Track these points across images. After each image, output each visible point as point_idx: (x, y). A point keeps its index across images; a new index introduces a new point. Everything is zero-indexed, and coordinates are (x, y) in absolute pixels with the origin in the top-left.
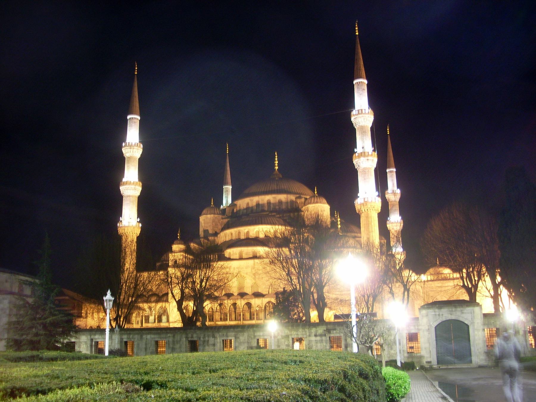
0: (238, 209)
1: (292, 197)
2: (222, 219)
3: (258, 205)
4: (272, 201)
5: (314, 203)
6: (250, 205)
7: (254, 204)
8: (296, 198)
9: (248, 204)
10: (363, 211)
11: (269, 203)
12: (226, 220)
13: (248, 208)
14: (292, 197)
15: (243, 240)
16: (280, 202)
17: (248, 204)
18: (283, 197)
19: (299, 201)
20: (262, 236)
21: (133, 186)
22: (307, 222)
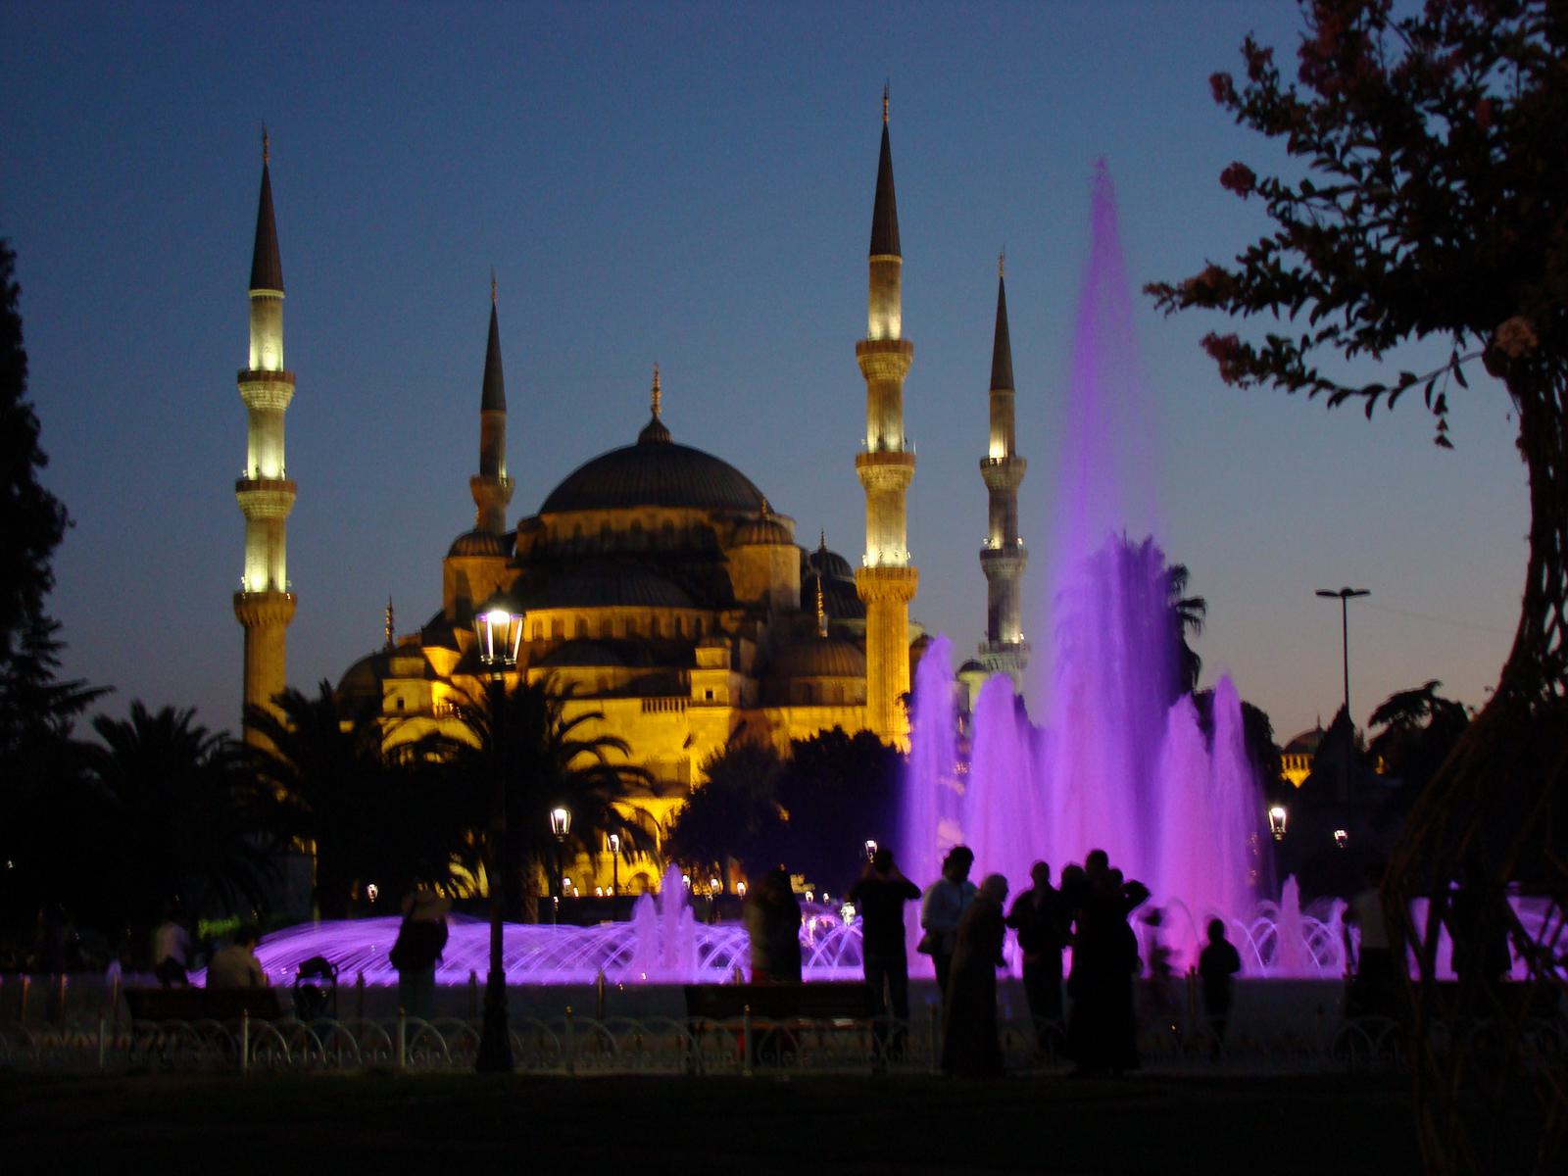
0: (549, 536)
1: (702, 516)
2: (508, 567)
3: (605, 531)
4: (646, 524)
5: (758, 543)
6: (585, 532)
7: (596, 529)
8: (714, 518)
9: (578, 528)
10: (873, 597)
11: (636, 528)
12: (515, 574)
13: (577, 539)
14: (702, 516)
15: (571, 643)
16: (668, 528)
17: (578, 528)
18: (675, 516)
19: (718, 529)
20: (618, 632)
21: (276, 494)
22: (738, 595)
